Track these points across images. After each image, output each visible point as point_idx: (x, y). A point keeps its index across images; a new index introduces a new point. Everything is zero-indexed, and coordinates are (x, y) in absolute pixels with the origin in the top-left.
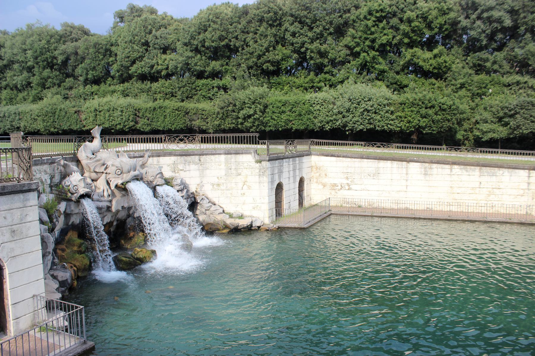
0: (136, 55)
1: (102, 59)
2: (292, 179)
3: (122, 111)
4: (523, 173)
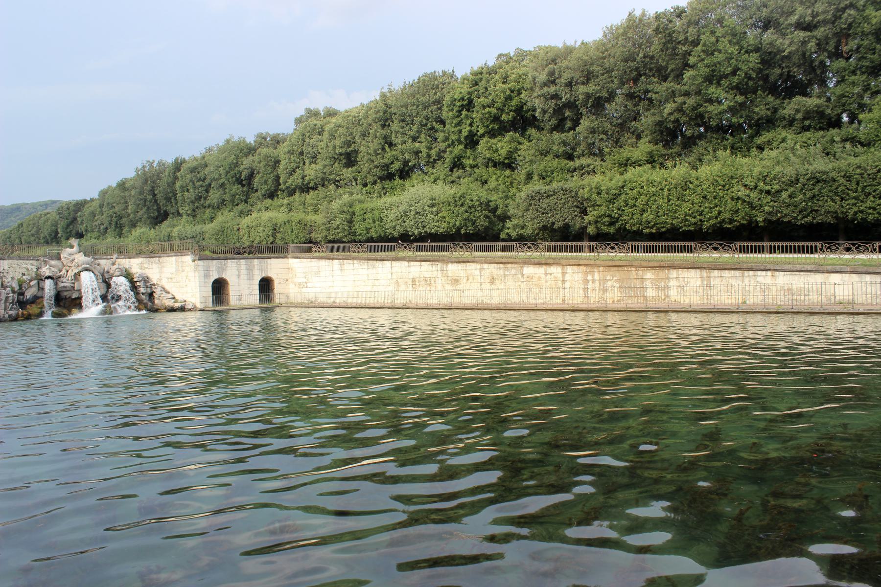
0: (293, 165)
1: (272, 172)
2: (244, 277)
3: (265, 226)
4: (388, 263)
